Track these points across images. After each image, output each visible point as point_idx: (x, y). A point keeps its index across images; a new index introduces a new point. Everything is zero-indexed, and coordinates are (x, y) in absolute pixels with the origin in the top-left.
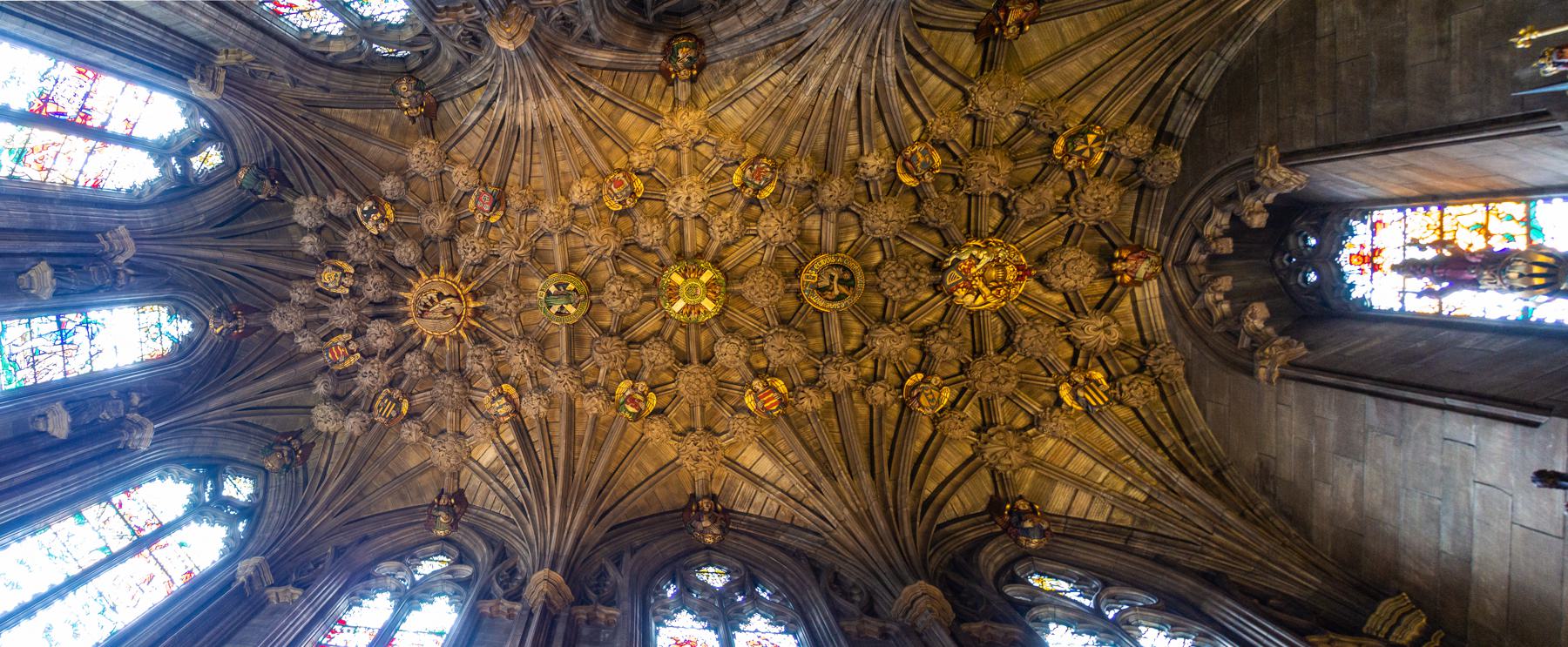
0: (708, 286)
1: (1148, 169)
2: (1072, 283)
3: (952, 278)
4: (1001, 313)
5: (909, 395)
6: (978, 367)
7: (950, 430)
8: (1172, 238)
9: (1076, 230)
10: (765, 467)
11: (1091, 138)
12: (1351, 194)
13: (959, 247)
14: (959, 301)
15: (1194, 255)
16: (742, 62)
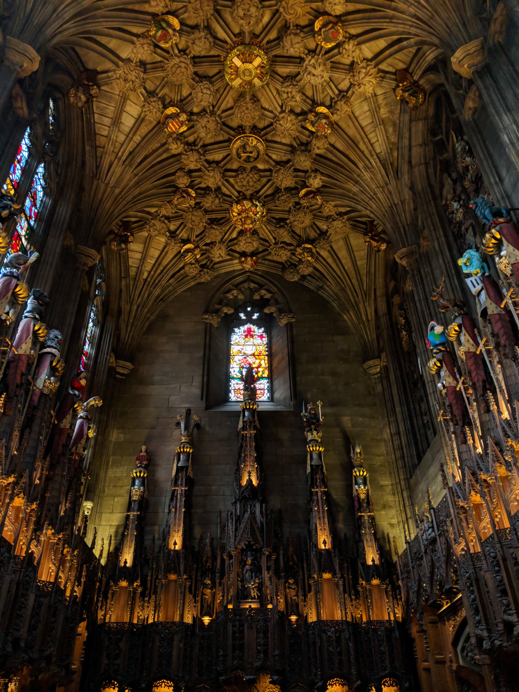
0: (250, 83)
1: (292, 270)
2: (242, 244)
3: (247, 204)
4: (228, 220)
5: (184, 191)
6: (200, 213)
7: (166, 209)
8: (261, 276)
9: (267, 244)
10: (128, 122)
11: (310, 259)
12: (273, 333)
13: (263, 206)
14: (234, 205)
15: (252, 285)
16: (394, 125)
